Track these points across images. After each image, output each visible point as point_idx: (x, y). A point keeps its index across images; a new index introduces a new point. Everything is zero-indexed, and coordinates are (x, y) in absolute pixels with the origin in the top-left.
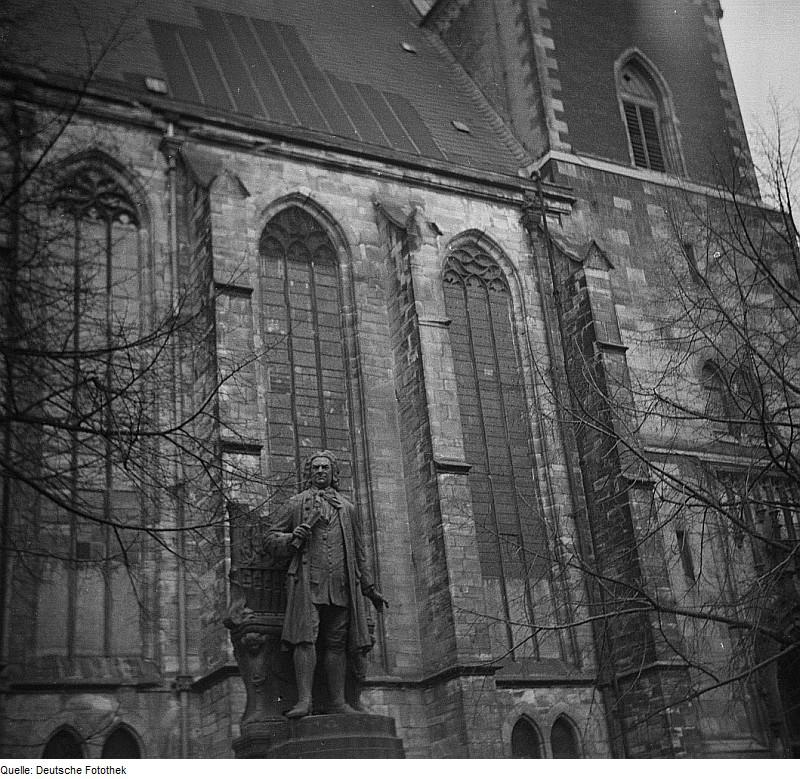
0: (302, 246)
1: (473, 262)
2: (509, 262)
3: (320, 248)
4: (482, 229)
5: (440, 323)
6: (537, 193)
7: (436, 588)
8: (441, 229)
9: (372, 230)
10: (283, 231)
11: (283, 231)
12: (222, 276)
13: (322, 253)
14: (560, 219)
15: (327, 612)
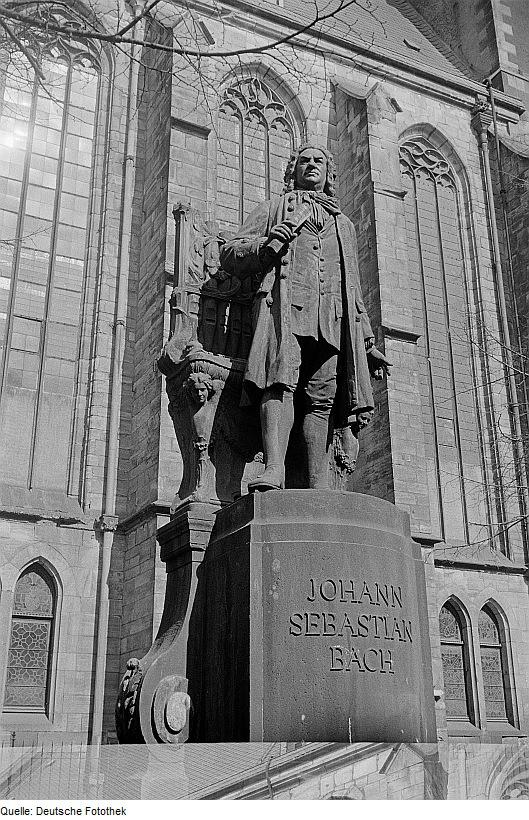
0: (259, 115)
1: (423, 156)
2: (457, 161)
3: (277, 119)
4: (434, 125)
5: (394, 193)
6: (489, 100)
7: (376, 455)
8: (400, 105)
9: (326, 110)
10: (243, 99)
11: (243, 99)
12: (174, 113)
13: (279, 125)
14: (508, 127)
15: (314, 351)
